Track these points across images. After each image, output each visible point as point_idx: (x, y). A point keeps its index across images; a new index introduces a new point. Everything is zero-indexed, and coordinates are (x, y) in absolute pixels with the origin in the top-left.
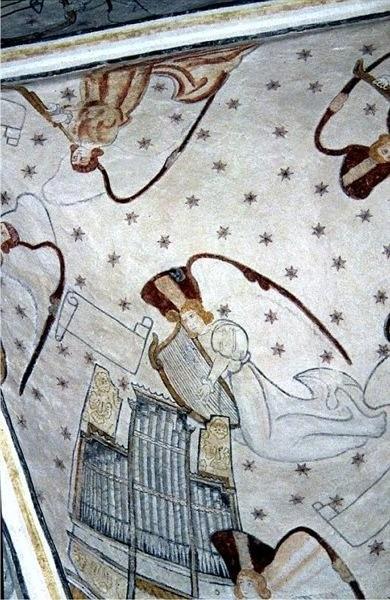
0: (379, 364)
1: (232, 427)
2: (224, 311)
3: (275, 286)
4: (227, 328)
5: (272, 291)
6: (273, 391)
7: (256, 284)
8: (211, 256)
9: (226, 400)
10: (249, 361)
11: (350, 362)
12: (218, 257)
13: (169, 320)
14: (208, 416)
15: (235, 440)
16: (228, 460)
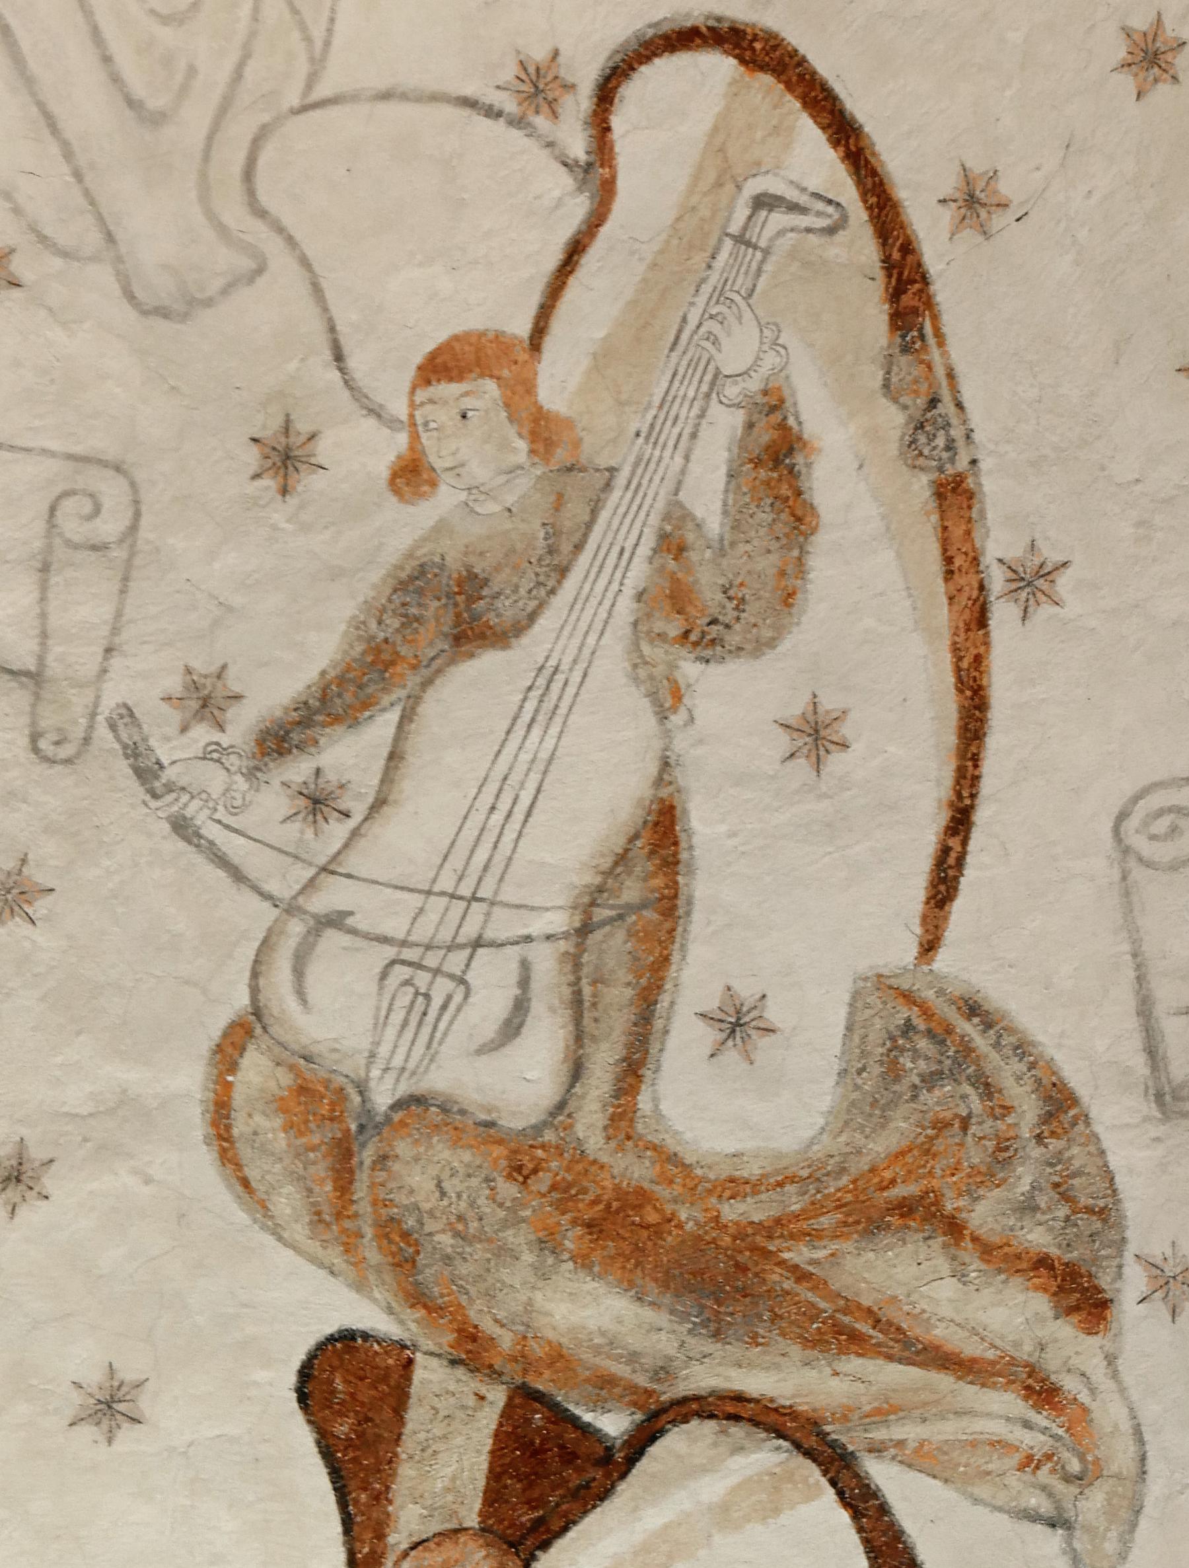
0: (469, 103)
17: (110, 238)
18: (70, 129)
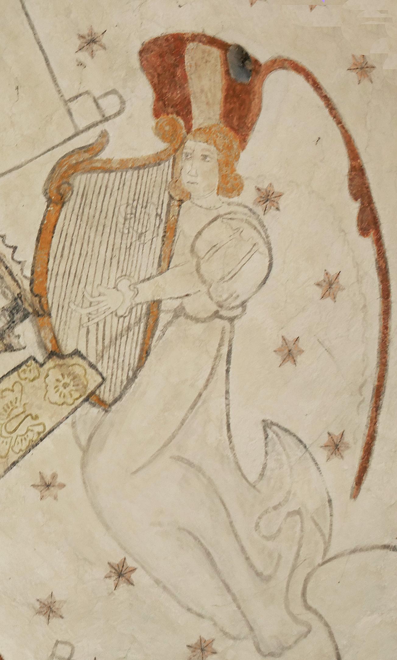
0: (386, 547)
1: (92, 398)
2: (268, 198)
3: (379, 242)
4: (248, 232)
5: (367, 244)
6: (216, 404)
7: (355, 207)
8: (316, 86)
9: (130, 350)
10: (231, 320)
11: (355, 495)
12: (326, 99)
13: (160, 132)
14: (68, 347)
15: (73, 424)
16: (24, 445)
17: (251, 629)
18: (234, 590)
